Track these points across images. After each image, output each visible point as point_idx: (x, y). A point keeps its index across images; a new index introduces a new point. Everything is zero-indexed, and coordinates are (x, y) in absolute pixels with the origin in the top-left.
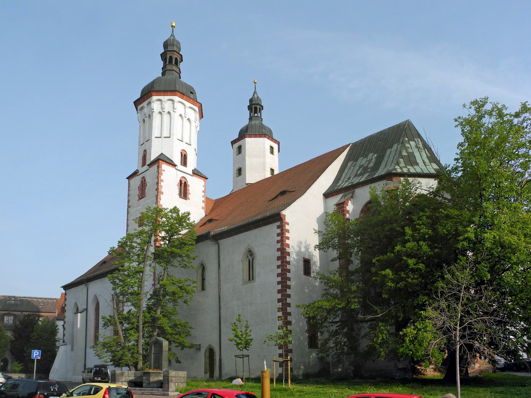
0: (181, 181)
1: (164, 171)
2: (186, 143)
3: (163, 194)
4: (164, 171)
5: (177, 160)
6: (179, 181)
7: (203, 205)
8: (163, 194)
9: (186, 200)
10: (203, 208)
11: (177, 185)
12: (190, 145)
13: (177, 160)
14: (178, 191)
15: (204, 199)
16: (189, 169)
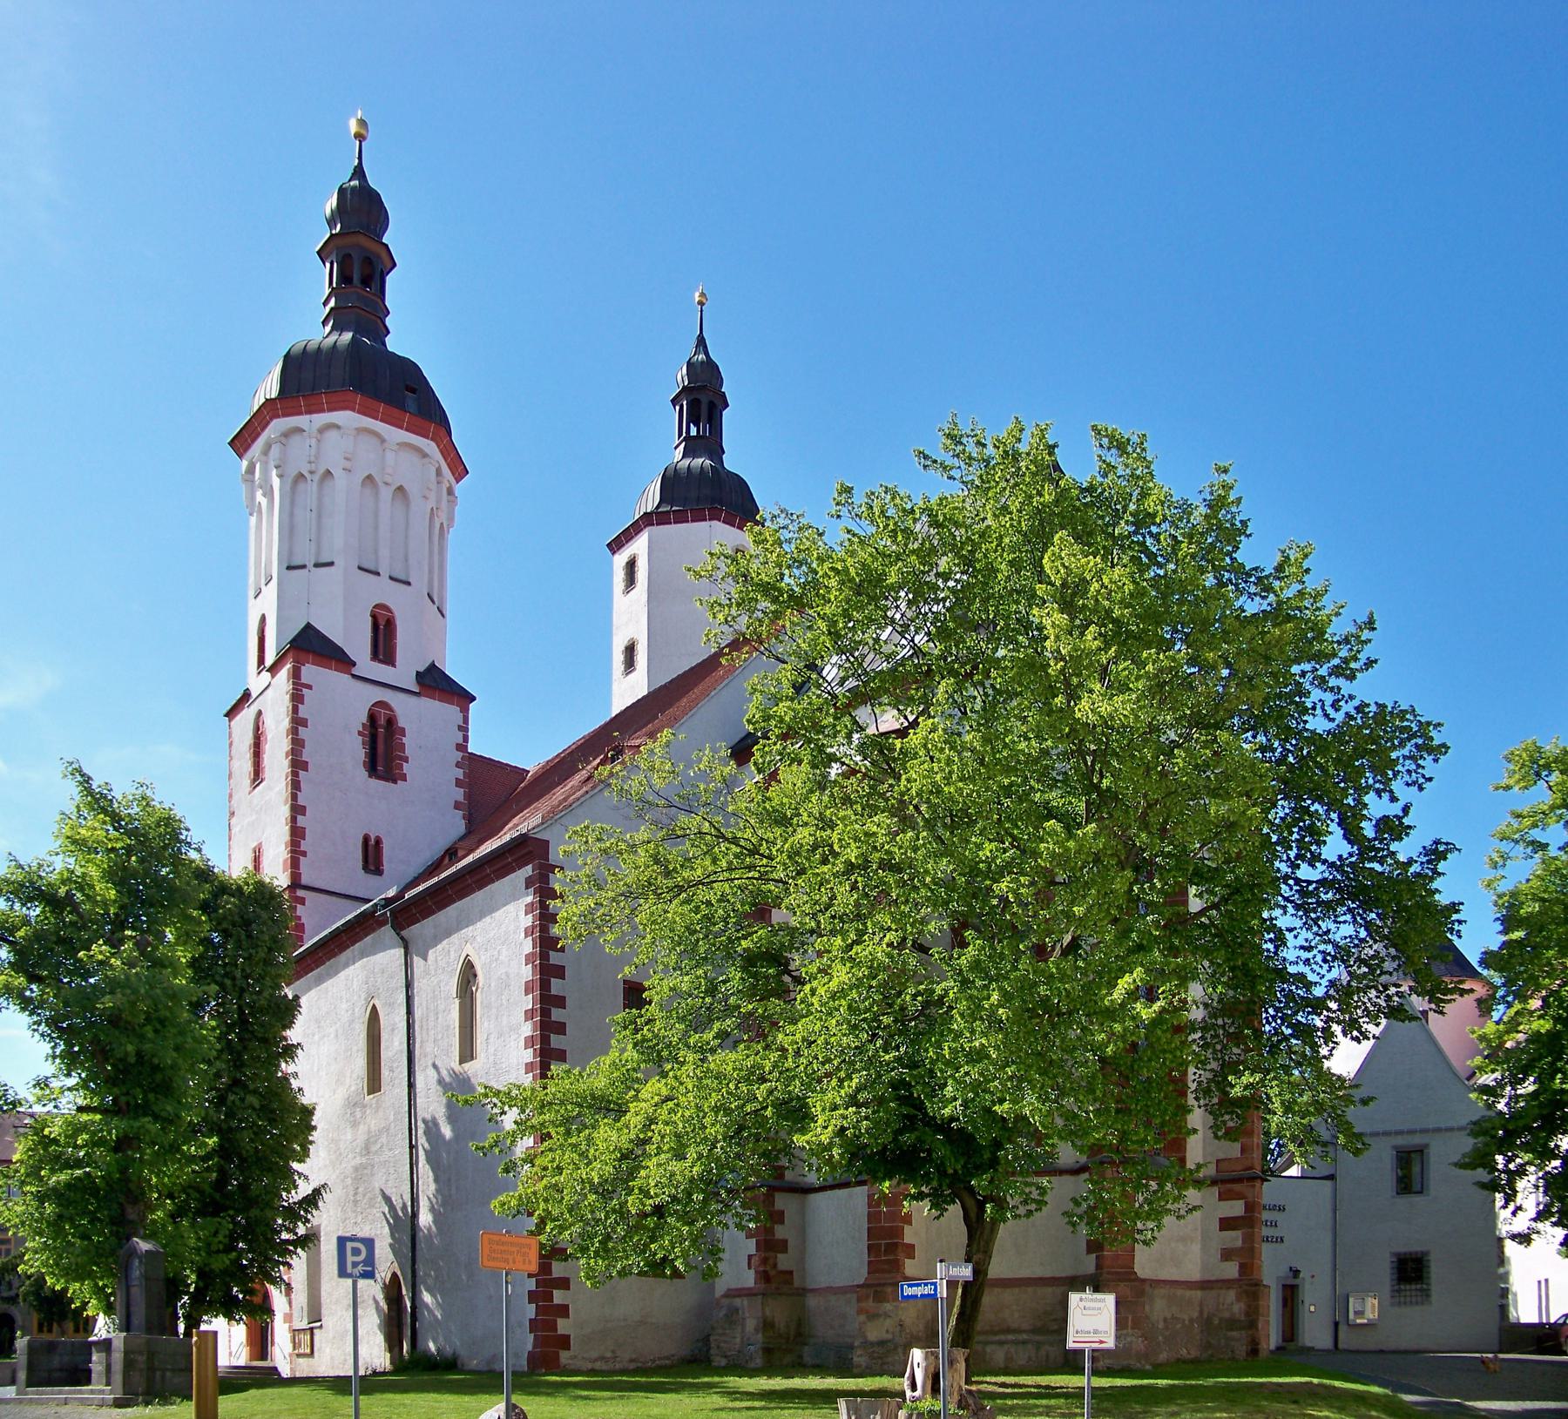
0: (372, 717)
1: (309, 687)
2: (391, 578)
3: (306, 770)
4: (309, 687)
5: (358, 645)
6: (364, 718)
7: (459, 794)
8: (306, 770)
9: (395, 782)
10: (457, 806)
11: (360, 733)
12: (409, 584)
13: (358, 645)
14: (361, 754)
15: (460, 773)
16: (404, 672)
